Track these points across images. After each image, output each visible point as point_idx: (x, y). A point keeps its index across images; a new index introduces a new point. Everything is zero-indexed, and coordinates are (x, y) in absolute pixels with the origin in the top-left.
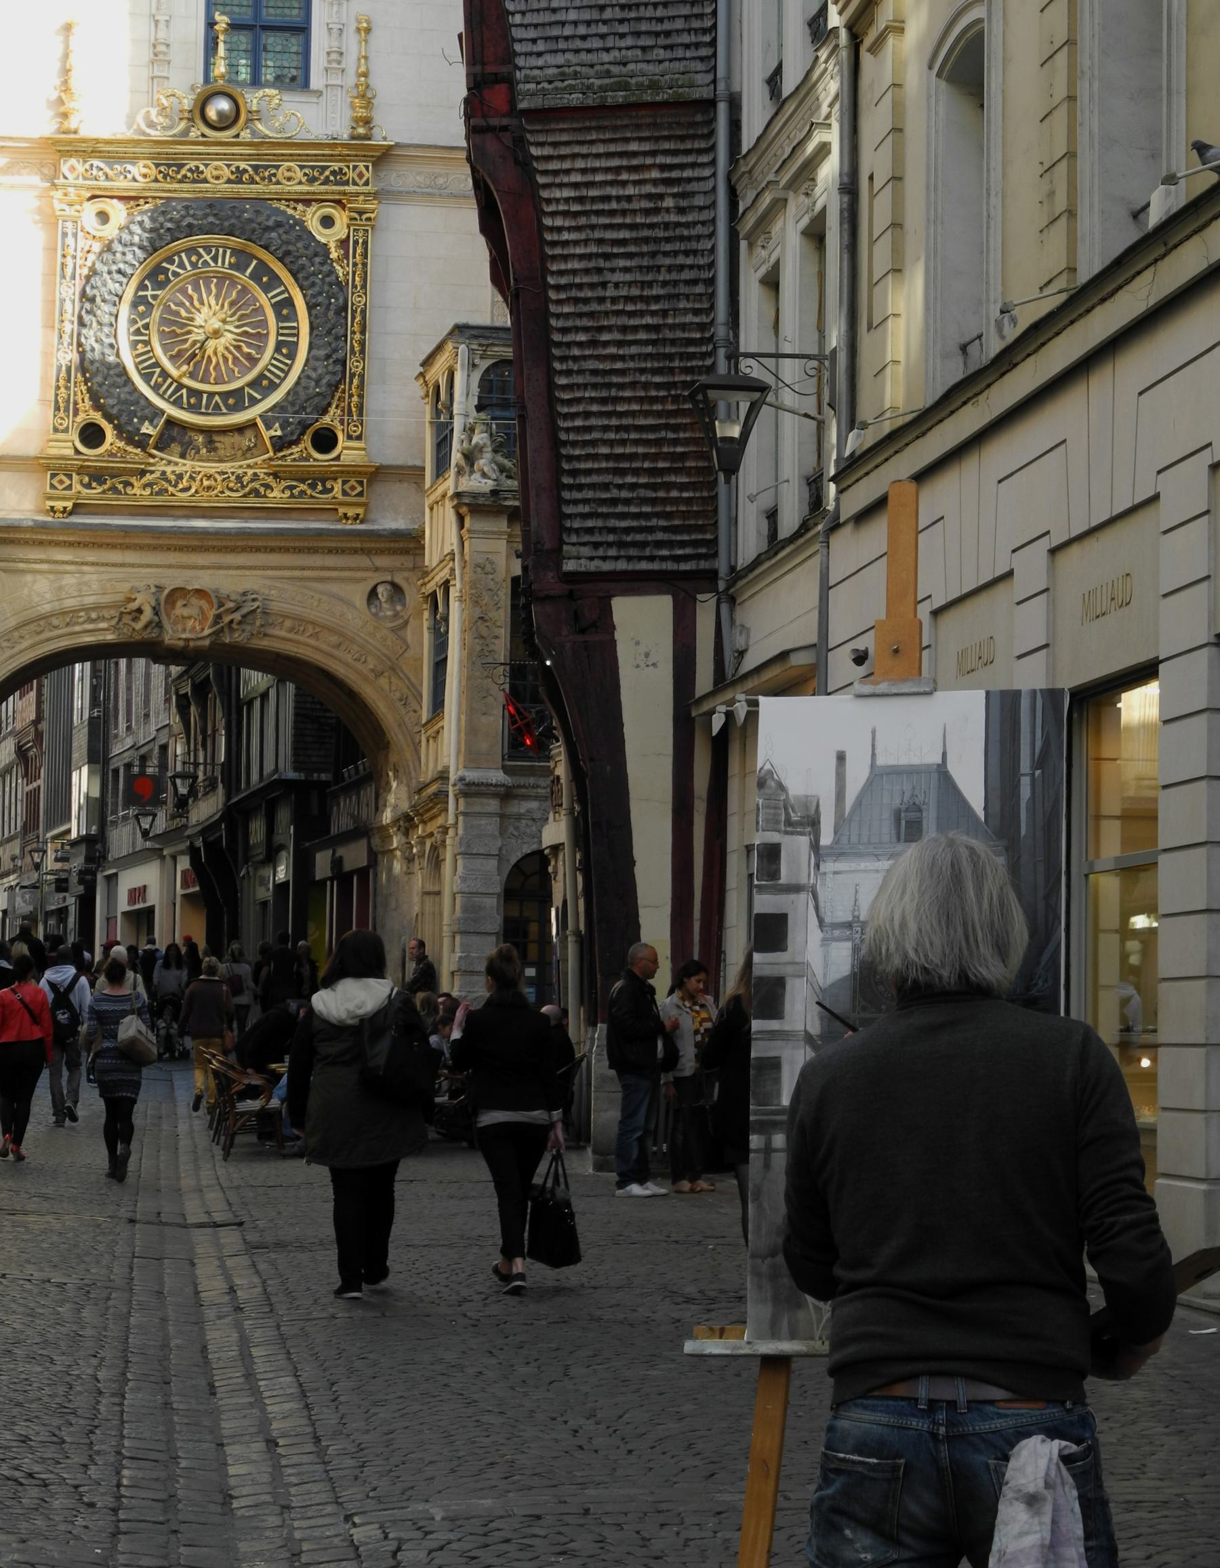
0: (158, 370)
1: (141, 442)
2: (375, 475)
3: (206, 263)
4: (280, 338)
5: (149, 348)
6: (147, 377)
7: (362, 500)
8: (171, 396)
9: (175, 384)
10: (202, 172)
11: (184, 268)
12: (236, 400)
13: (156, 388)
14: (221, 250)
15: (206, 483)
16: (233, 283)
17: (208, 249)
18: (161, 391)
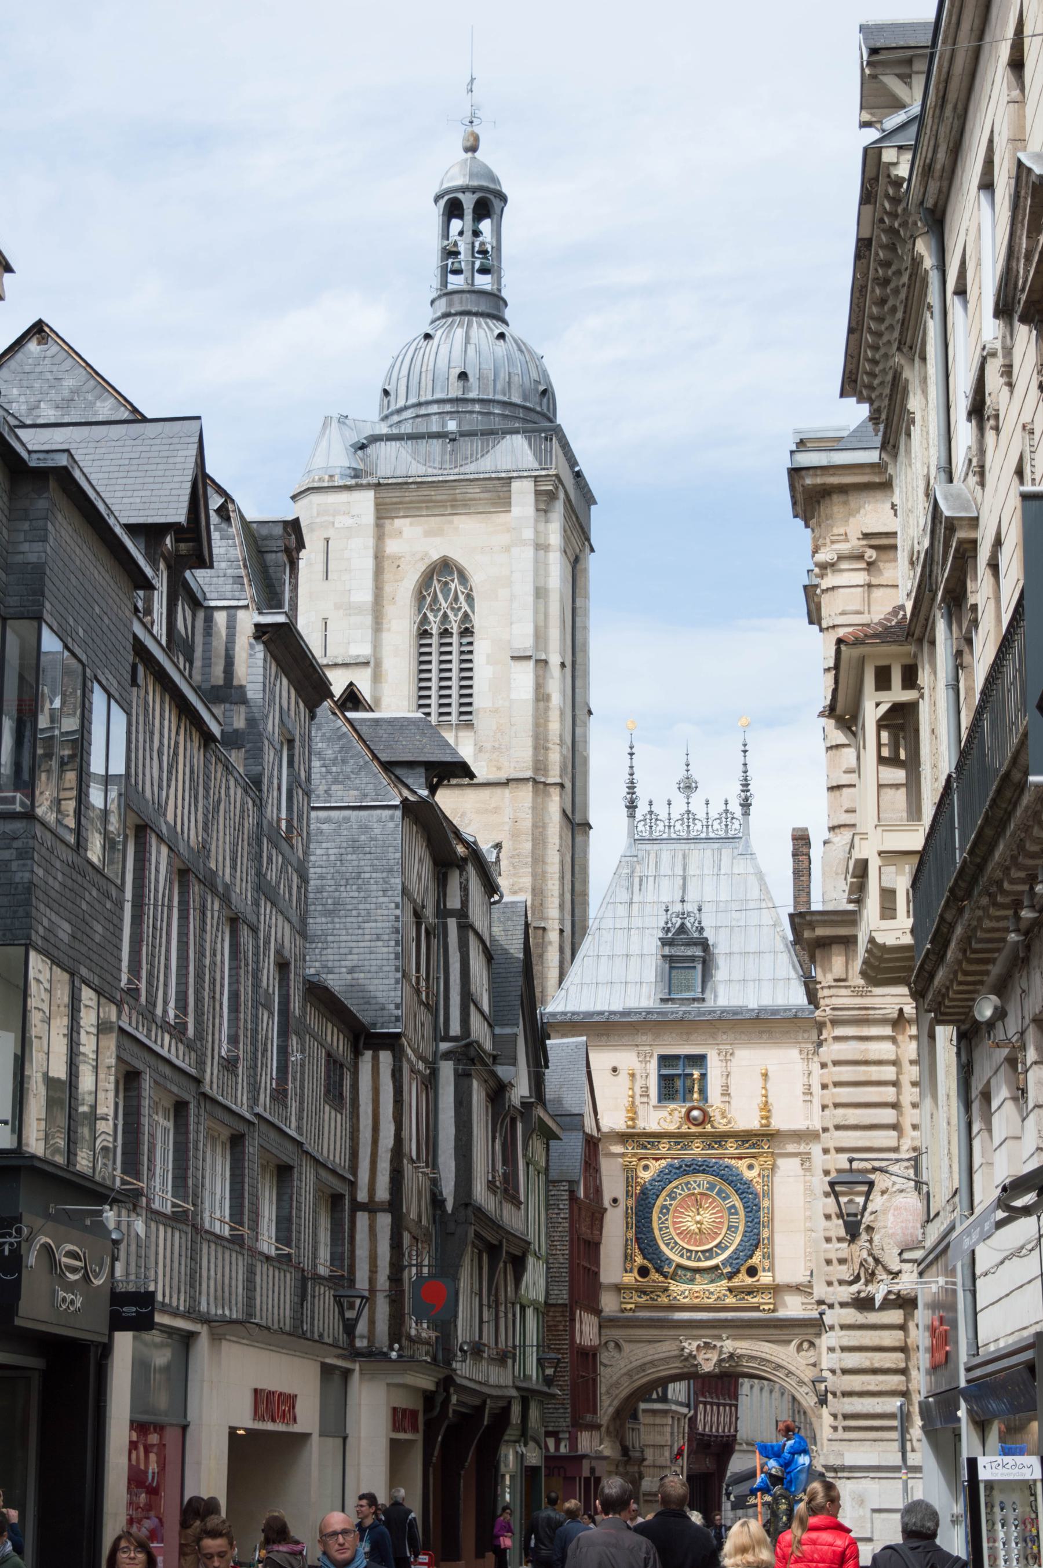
2: (776, 1289)
6: (667, 1245)
12: (709, 1254)
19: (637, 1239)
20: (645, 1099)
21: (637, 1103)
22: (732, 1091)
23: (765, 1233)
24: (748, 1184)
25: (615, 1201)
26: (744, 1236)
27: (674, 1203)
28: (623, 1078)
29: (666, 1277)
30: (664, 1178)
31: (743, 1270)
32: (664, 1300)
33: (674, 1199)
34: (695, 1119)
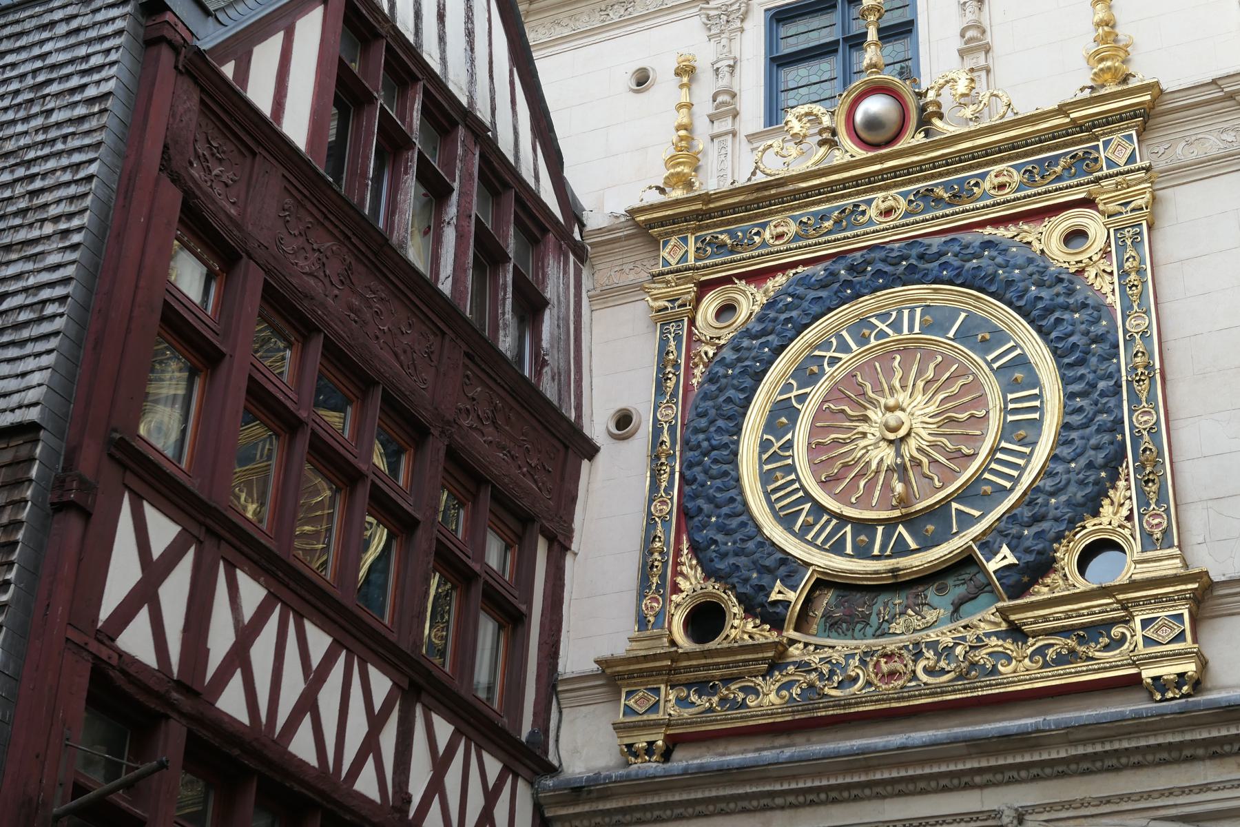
0: (807, 506)
1: (773, 617)
2: (1204, 598)
3: (882, 334)
4: (1010, 418)
5: (793, 476)
6: (787, 521)
7: (1188, 644)
8: (824, 542)
9: (834, 521)
10: (863, 213)
11: (847, 349)
13: (801, 536)
14: (906, 312)
15: (885, 668)
16: (929, 355)
17: (883, 317)
18: (809, 537)
19: (685, 513)
20: (725, 125)
21: (701, 143)
22: (996, 38)
23: (1133, 420)
24: (1068, 282)
25: (624, 420)
26: (1061, 441)
27: (817, 392)
28: (666, 88)
29: (777, 623)
30: (777, 327)
31: (1067, 557)
32: (770, 698)
33: (813, 379)
34: (873, 123)
